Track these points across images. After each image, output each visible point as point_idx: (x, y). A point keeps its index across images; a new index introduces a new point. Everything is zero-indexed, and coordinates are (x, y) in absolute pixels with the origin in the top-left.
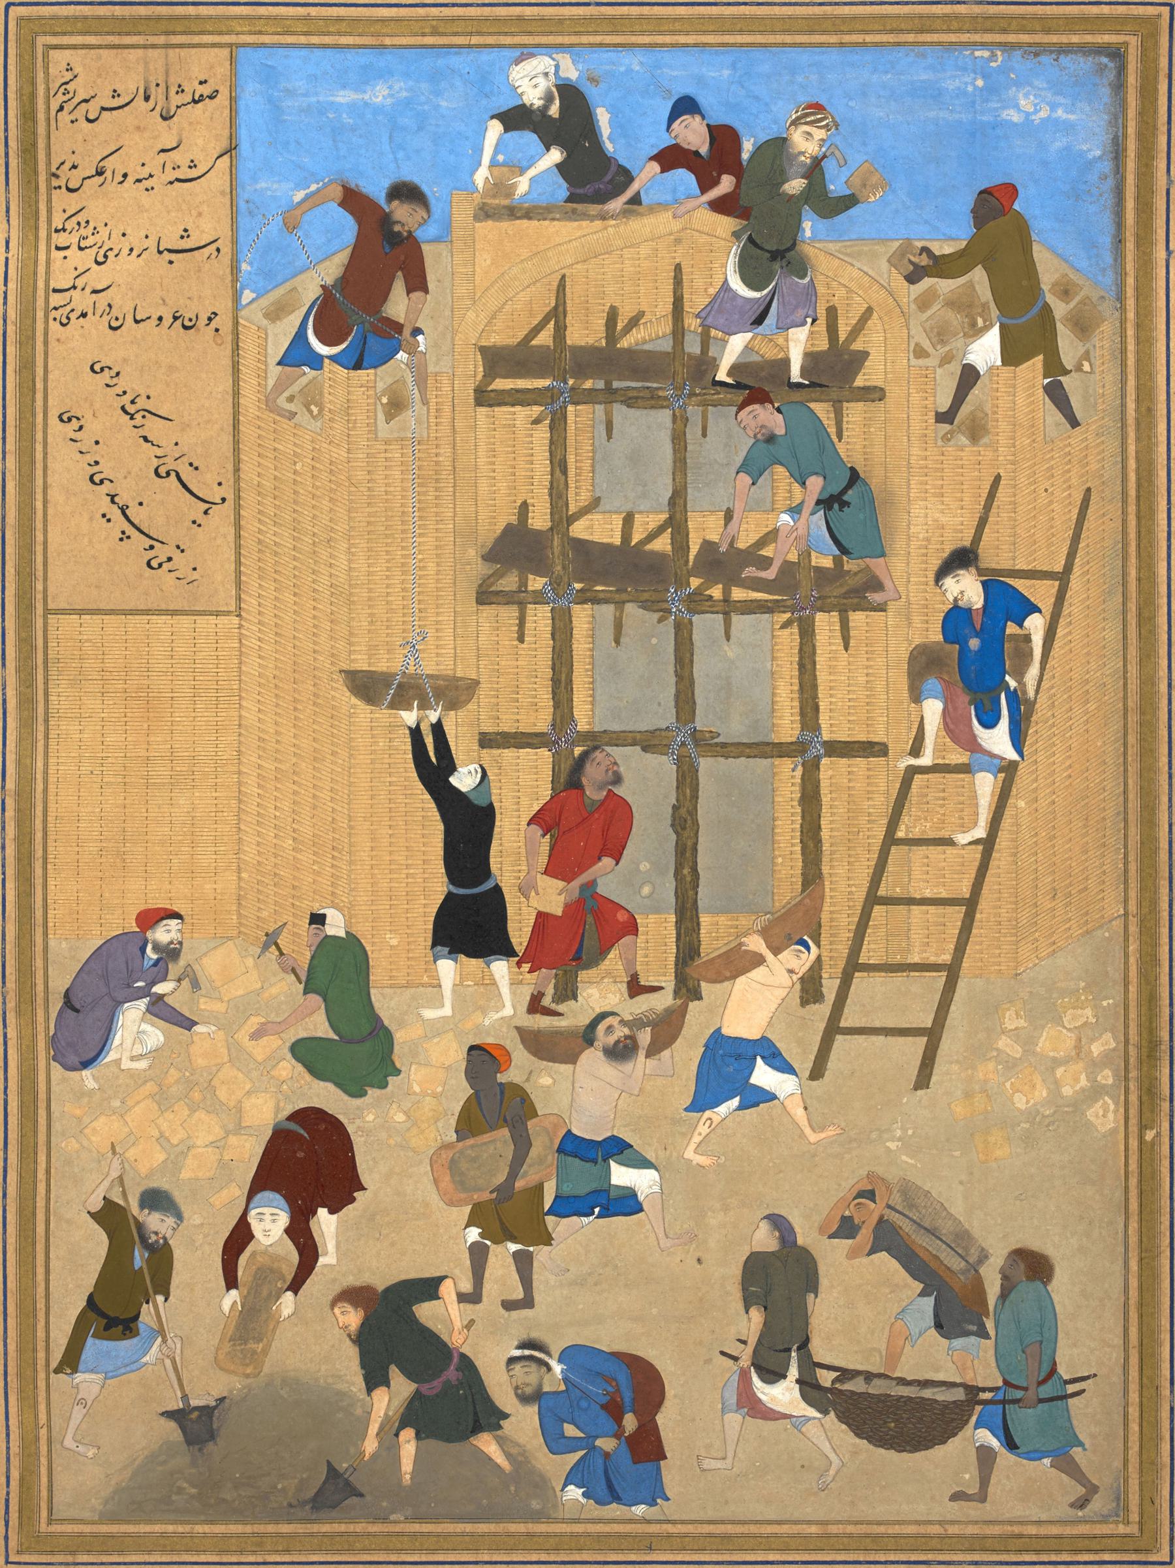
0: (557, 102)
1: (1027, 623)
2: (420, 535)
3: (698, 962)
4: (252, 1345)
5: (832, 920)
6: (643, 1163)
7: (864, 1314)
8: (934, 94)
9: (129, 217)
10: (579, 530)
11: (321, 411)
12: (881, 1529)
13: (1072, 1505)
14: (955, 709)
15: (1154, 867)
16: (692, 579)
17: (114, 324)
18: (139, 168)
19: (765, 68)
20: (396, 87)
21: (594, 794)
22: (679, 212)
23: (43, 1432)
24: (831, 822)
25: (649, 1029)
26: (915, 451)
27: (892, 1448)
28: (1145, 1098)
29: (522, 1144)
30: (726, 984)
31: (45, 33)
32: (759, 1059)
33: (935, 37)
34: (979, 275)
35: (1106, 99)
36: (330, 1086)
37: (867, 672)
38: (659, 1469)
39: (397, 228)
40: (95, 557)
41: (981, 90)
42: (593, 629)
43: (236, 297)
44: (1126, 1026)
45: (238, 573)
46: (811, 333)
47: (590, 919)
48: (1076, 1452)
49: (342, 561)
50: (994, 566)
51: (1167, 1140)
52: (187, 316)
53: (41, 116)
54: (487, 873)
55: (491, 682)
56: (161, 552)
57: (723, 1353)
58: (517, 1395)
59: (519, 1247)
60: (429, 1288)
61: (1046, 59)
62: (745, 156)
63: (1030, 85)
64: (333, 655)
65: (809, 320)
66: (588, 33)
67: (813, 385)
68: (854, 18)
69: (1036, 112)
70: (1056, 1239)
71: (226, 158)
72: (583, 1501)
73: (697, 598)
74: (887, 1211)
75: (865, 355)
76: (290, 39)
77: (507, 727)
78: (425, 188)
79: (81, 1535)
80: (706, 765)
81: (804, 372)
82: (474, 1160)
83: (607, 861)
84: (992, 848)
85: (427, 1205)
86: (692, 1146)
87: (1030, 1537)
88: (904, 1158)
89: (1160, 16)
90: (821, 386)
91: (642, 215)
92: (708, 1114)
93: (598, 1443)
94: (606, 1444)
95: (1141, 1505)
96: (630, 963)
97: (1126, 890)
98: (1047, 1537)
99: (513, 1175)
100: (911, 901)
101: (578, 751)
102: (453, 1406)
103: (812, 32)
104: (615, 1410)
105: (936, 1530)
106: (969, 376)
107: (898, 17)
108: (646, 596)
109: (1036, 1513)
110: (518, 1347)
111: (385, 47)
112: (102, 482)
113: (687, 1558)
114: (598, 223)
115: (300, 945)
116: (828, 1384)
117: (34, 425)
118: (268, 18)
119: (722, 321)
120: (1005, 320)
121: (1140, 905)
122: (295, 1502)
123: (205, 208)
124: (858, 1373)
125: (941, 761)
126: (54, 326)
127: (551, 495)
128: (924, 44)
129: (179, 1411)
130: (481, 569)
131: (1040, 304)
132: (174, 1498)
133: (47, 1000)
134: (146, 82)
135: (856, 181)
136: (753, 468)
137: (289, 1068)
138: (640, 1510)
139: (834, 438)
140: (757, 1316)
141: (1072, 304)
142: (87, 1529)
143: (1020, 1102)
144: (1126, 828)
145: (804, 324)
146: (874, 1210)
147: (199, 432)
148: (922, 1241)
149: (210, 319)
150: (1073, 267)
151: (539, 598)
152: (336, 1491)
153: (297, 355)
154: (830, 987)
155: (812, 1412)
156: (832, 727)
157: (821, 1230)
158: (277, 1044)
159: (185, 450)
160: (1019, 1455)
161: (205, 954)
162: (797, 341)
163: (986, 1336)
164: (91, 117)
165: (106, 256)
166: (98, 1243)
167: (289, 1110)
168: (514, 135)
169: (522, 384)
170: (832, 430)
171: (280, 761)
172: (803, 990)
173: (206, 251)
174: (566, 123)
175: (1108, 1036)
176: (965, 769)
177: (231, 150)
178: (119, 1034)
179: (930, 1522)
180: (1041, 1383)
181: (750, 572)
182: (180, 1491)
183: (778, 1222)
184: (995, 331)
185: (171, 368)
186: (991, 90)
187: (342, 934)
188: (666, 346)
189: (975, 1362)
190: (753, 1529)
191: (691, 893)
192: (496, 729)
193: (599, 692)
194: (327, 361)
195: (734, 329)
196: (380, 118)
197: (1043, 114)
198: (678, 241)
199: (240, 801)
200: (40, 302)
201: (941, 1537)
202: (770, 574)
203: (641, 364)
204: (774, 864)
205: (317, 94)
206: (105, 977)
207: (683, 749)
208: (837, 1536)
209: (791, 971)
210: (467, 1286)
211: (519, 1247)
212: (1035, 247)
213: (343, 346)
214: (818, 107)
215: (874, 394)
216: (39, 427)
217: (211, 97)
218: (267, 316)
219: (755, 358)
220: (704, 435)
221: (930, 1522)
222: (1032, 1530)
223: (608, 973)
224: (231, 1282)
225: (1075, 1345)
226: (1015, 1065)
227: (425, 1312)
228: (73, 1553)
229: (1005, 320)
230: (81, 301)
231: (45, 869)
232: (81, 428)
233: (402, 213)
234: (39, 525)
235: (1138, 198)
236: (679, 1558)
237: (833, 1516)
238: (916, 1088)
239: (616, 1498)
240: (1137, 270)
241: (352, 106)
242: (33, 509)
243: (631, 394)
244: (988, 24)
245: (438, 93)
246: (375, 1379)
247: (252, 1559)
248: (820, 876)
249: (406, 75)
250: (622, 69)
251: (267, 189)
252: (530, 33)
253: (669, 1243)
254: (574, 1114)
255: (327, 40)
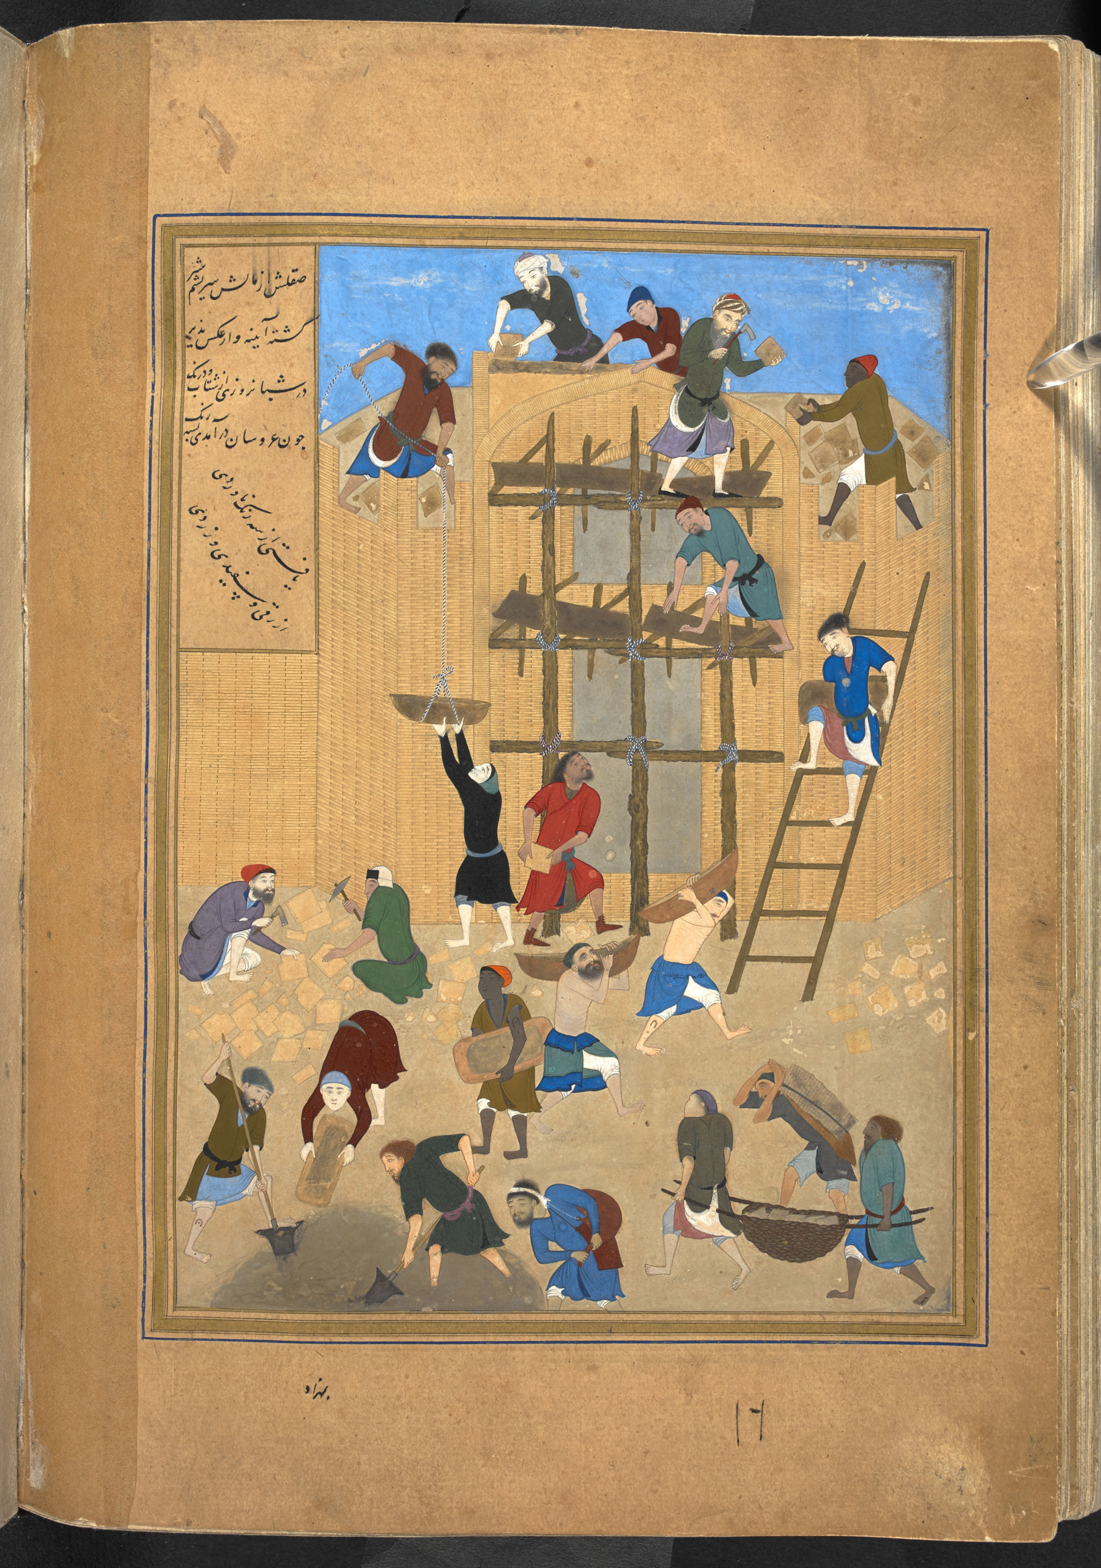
0: (549, 288)
1: (884, 668)
2: (449, 598)
3: (647, 908)
4: (322, 1183)
5: (743, 879)
6: (607, 1053)
7: (766, 1162)
8: (819, 291)
9: (243, 366)
10: (563, 596)
11: (377, 507)
12: (778, 1318)
13: (915, 1302)
14: (832, 728)
15: (975, 843)
16: (644, 633)
17: (230, 444)
18: (249, 332)
19: (698, 268)
20: (434, 275)
21: (572, 786)
22: (636, 370)
23: (171, 1243)
24: (743, 808)
25: (611, 956)
26: (804, 544)
27: (785, 1259)
28: (968, 1009)
29: (520, 1039)
30: (667, 924)
31: (182, 236)
32: (691, 979)
33: (819, 250)
34: (850, 420)
35: (941, 297)
36: (381, 995)
37: (769, 700)
38: (617, 1274)
39: (433, 377)
40: (214, 611)
41: (852, 288)
42: (572, 667)
43: (318, 424)
44: (955, 957)
45: (317, 623)
46: (730, 458)
47: (569, 876)
48: (918, 1263)
49: (392, 616)
50: (860, 627)
51: (984, 1040)
52: (282, 438)
53: (178, 295)
54: (495, 843)
55: (499, 705)
56: (262, 608)
57: (664, 1190)
58: (515, 1221)
59: (517, 1113)
60: (451, 1143)
61: (897, 267)
62: (683, 330)
63: (887, 285)
64: (385, 683)
65: (729, 449)
66: (571, 240)
67: (731, 495)
68: (761, 235)
69: (891, 304)
70: (904, 1109)
71: (311, 325)
72: (562, 1297)
73: (648, 646)
74: (783, 1088)
75: (769, 474)
76: (357, 240)
77: (510, 737)
78: (453, 348)
79: (197, 1318)
80: (654, 767)
81: (725, 486)
82: (485, 1050)
83: (582, 835)
84: (859, 829)
85: (450, 1082)
86: (642, 1041)
87: (885, 1324)
88: (795, 1050)
89: (979, 238)
90: (737, 496)
91: (609, 371)
92: (653, 1017)
93: (573, 1255)
94: (579, 1256)
95: (965, 1303)
96: (598, 908)
97: (955, 860)
98: (897, 1324)
99: (513, 1061)
100: (800, 866)
101: (561, 755)
102: (468, 1227)
103: (731, 243)
104: (585, 1231)
105: (817, 1318)
106: (843, 492)
107: (793, 235)
108: (611, 644)
109: (889, 1307)
110: (516, 1186)
111: (425, 246)
112: (219, 557)
113: (638, 1339)
114: (578, 376)
115: (360, 893)
116: (739, 1213)
117: (171, 516)
118: (342, 224)
119: (666, 448)
120: (868, 452)
121: (965, 871)
122: (353, 1298)
123: (295, 361)
124: (761, 1205)
125: (822, 766)
126: (186, 445)
127: (543, 570)
128: (811, 255)
129: (269, 1230)
130: (492, 623)
131: (893, 441)
132: (265, 1293)
133: (176, 930)
134: (254, 270)
135: (763, 351)
136: (688, 553)
137: (351, 982)
138: (603, 1304)
139: (746, 533)
140: (688, 1164)
141: (916, 442)
142: (202, 1314)
143: (879, 1011)
144: (954, 815)
145: (724, 451)
146: (774, 1087)
147: (290, 522)
148: (807, 1110)
149: (298, 440)
150: (917, 415)
151: (534, 644)
152: (383, 1290)
153: (361, 467)
154: (742, 927)
155: (728, 1233)
156: (744, 740)
157: (735, 1102)
158: (343, 965)
159: (280, 534)
160: (877, 1265)
161: (291, 899)
162: (720, 463)
163: (854, 1179)
164: (214, 296)
165: (224, 395)
166: (211, 1107)
167: (351, 1012)
168: (518, 311)
169: (522, 490)
170: (745, 528)
171: (347, 760)
172: (722, 929)
173: (296, 391)
174: (556, 304)
175: (942, 964)
176: (839, 771)
177: (315, 319)
178: (229, 955)
179: (813, 1313)
180: (893, 1213)
181: (685, 628)
182: (270, 1288)
183: (704, 1096)
184: (861, 461)
185: (271, 476)
186: (859, 289)
187: (390, 885)
188: (626, 465)
189: (845, 1197)
190: (685, 1317)
191: (642, 858)
192: (502, 739)
193: (576, 713)
194: (382, 471)
195: (674, 454)
196: (422, 297)
197: (896, 306)
198: (635, 390)
199: (317, 788)
200: (176, 428)
201: (821, 1324)
202: (700, 630)
203: (608, 478)
204: (702, 838)
205: (376, 279)
206: (219, 914)
207: (637, 755)
208: (746, 1323)
209: (714, 915)
210: (479, 1141)
211: (517, 1113)
212: (890, 401)
213: (394, 461)
214: (735, 297)
215: (775, 503)
216: (175, 517)
217: (300, 281)
218: (339, 438)
219: (690, 475)
220: (653, 529)
221: (813, 1313)
222: (887, 1319)
223: (582, 916)
224: (308, 1137)
225: (917, 1186)
226: (874, 984)
227: (449, 1160)
228: (192, 1331)
229: (868, 452)
230: (206, 427)
231: (176, 835)
232: (205, 518)
233: (437, 365)
234: (174, 588)
235: (963, 367)
236: (631, 1338)
237: (743, 1308)
238: (804, 1000)
239: (586, 1295)
240: (963, 418)
241: (402, 289)
242: (170, 576)
243: (601, 499)
244: (857, 242)
245: (463, 281)
246: (412, 1208)
247: (321, 1339)
248: (735, 847)
249: (441, 267)
250: (596, 266)
251: (341, 347)
252: (530, 239)
253: (625, 1111)
254: (557, 1017)
255: (384, 241)
